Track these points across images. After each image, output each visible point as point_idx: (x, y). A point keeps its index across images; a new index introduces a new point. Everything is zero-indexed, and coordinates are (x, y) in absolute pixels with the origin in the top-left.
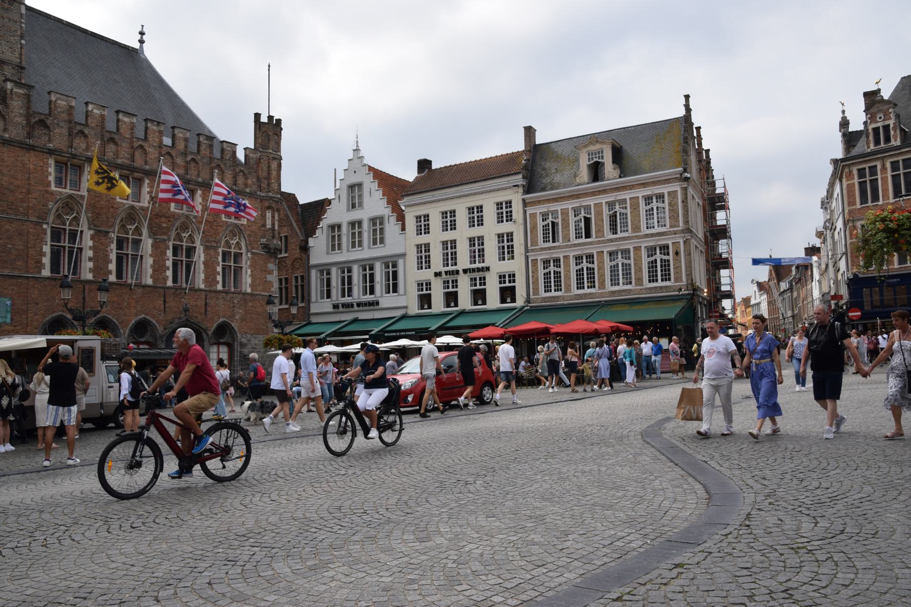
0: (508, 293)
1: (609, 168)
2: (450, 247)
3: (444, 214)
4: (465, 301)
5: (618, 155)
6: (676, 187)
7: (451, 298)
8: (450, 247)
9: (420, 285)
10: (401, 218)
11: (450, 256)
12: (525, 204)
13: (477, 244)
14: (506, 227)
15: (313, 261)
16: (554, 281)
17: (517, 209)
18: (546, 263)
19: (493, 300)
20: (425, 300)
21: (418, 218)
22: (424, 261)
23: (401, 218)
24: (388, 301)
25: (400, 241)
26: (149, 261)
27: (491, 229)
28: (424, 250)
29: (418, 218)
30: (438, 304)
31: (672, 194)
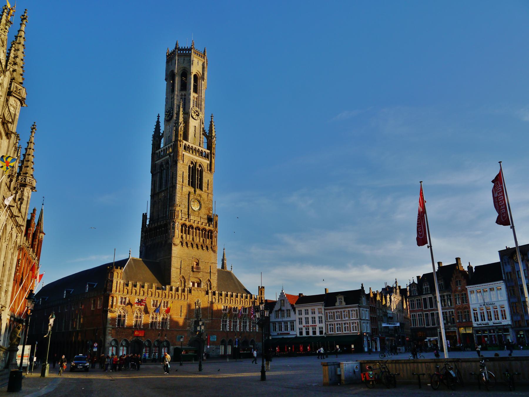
0: (321, 332)
2: (307, 319)
3: (306, 310)
4: (311, 334)
6: (357, 309)
7: (308, 333)
8: (307, 319)
9: (300, 329)
10: (294, 310)
11: (307, 322)
12: (325, 310)
14: (320, 315)
15: (271, 321)
16: (332, 330)
18: (330, 325)
19: (318, 334)
20: (301, 333)
21: (299, 311)
22: (301, 323)
24: (291, 333)
26: (238, 326)
27: (317, 315)
28: (300, 319)
29: (299, 311)
30: (304, 334)
31: (357, 310)
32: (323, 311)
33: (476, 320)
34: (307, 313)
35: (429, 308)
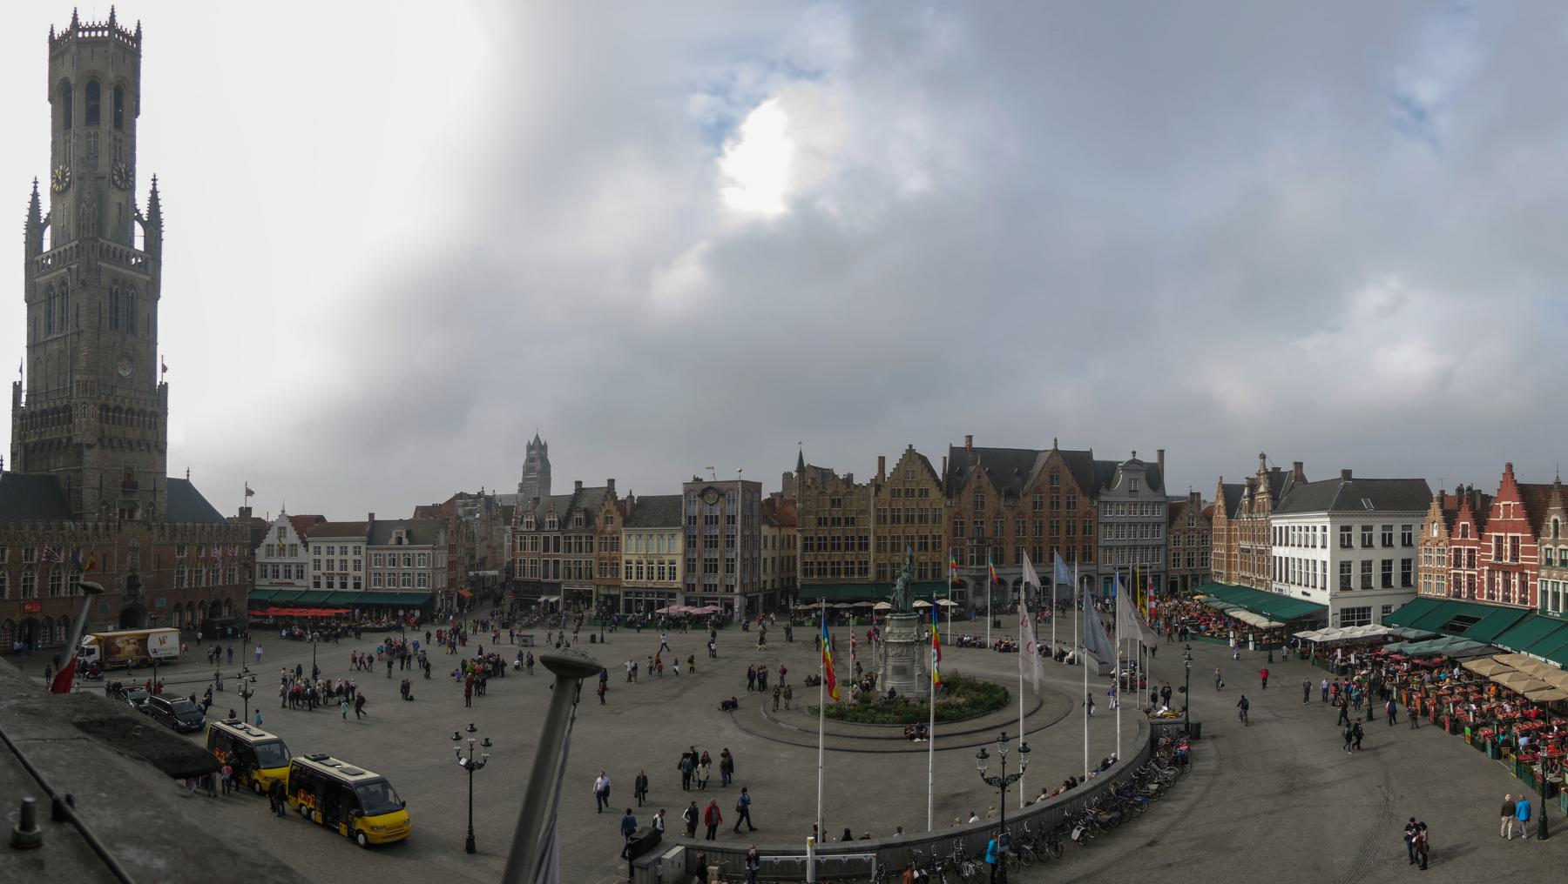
0: (357, 585)
1: (405, 541)
2: (330, 564)
4: (337, 587)
5: (409, 534)
7: (330, 585)
10: (306, 545)
13: (344, 564)
14: (357, 557)
17: (363, 550)
19: (350, 588)
20: (317, 584)
23: (306, 545)
24: (298, 582)
25: (304, 556)
27: (350, 557)
32: (363, 550)
33: (629, 576)
34: (331, 551)
35: (552, 552)
